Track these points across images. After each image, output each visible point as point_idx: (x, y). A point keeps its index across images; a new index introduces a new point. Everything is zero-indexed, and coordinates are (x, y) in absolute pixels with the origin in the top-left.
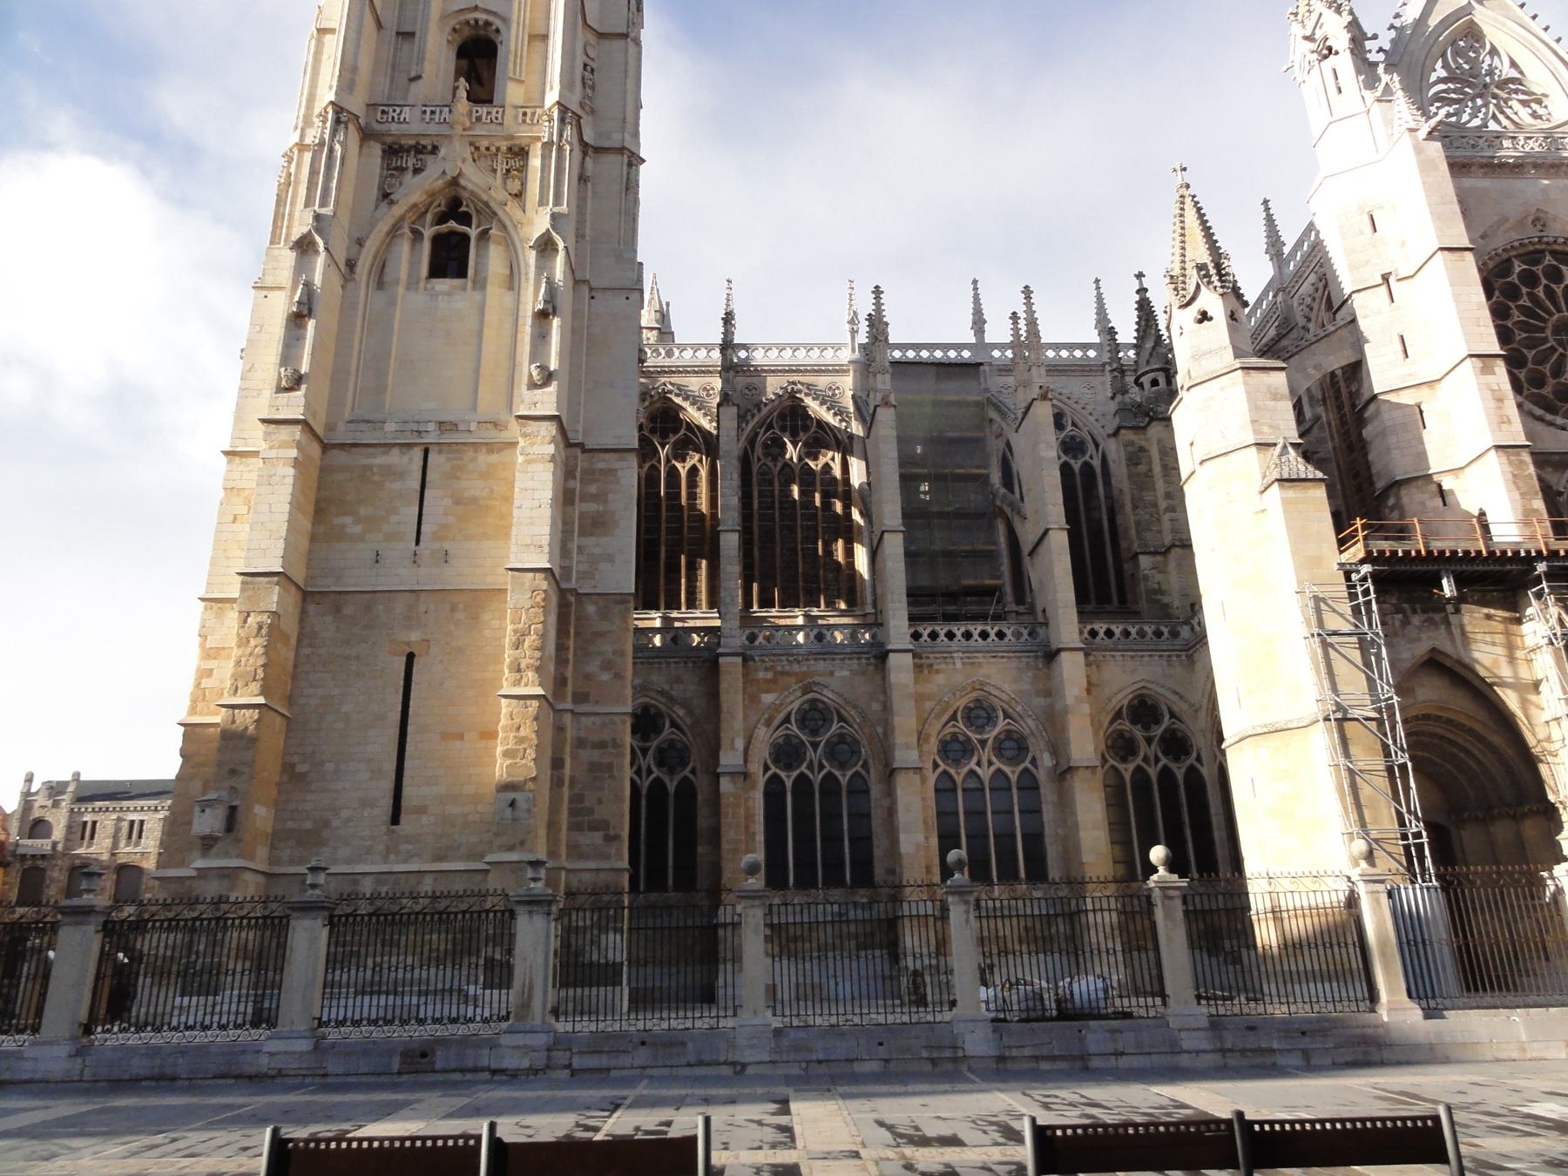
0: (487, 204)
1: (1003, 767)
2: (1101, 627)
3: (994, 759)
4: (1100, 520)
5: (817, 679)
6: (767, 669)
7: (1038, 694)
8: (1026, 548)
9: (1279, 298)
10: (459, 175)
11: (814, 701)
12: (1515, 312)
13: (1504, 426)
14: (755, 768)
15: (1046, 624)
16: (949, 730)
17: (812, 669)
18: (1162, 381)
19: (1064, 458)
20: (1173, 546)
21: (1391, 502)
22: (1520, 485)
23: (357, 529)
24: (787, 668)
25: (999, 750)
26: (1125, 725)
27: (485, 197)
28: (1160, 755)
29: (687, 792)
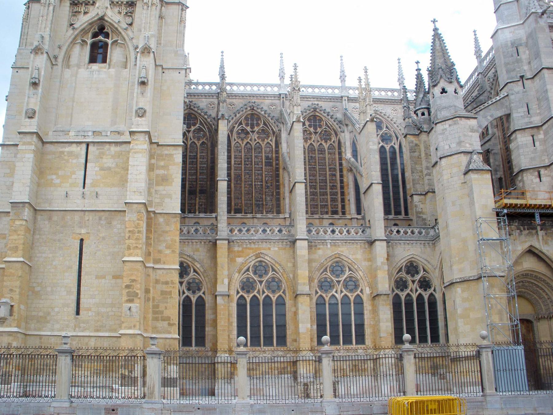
0: (117, 29)
1: (348, 294)
3: (343, 290)
4: (397, 175)
5: (262, 251)
6: (239, 246)
7: (365, 260)
8: (362, 191)
10: (104, 16)
11: (261, 261)
14: (233, 292)
15: (370, 227)
17: (260, 246)
18: (426, 113)
19: (382, 144)
20: (429, 192)
21: (520, 178)
23: (58, 181)
24: (249, 246)
25: (346, 286)
26: (403, 274)
27: (116, 26)
28: (418, 288)
29: (201, 302)
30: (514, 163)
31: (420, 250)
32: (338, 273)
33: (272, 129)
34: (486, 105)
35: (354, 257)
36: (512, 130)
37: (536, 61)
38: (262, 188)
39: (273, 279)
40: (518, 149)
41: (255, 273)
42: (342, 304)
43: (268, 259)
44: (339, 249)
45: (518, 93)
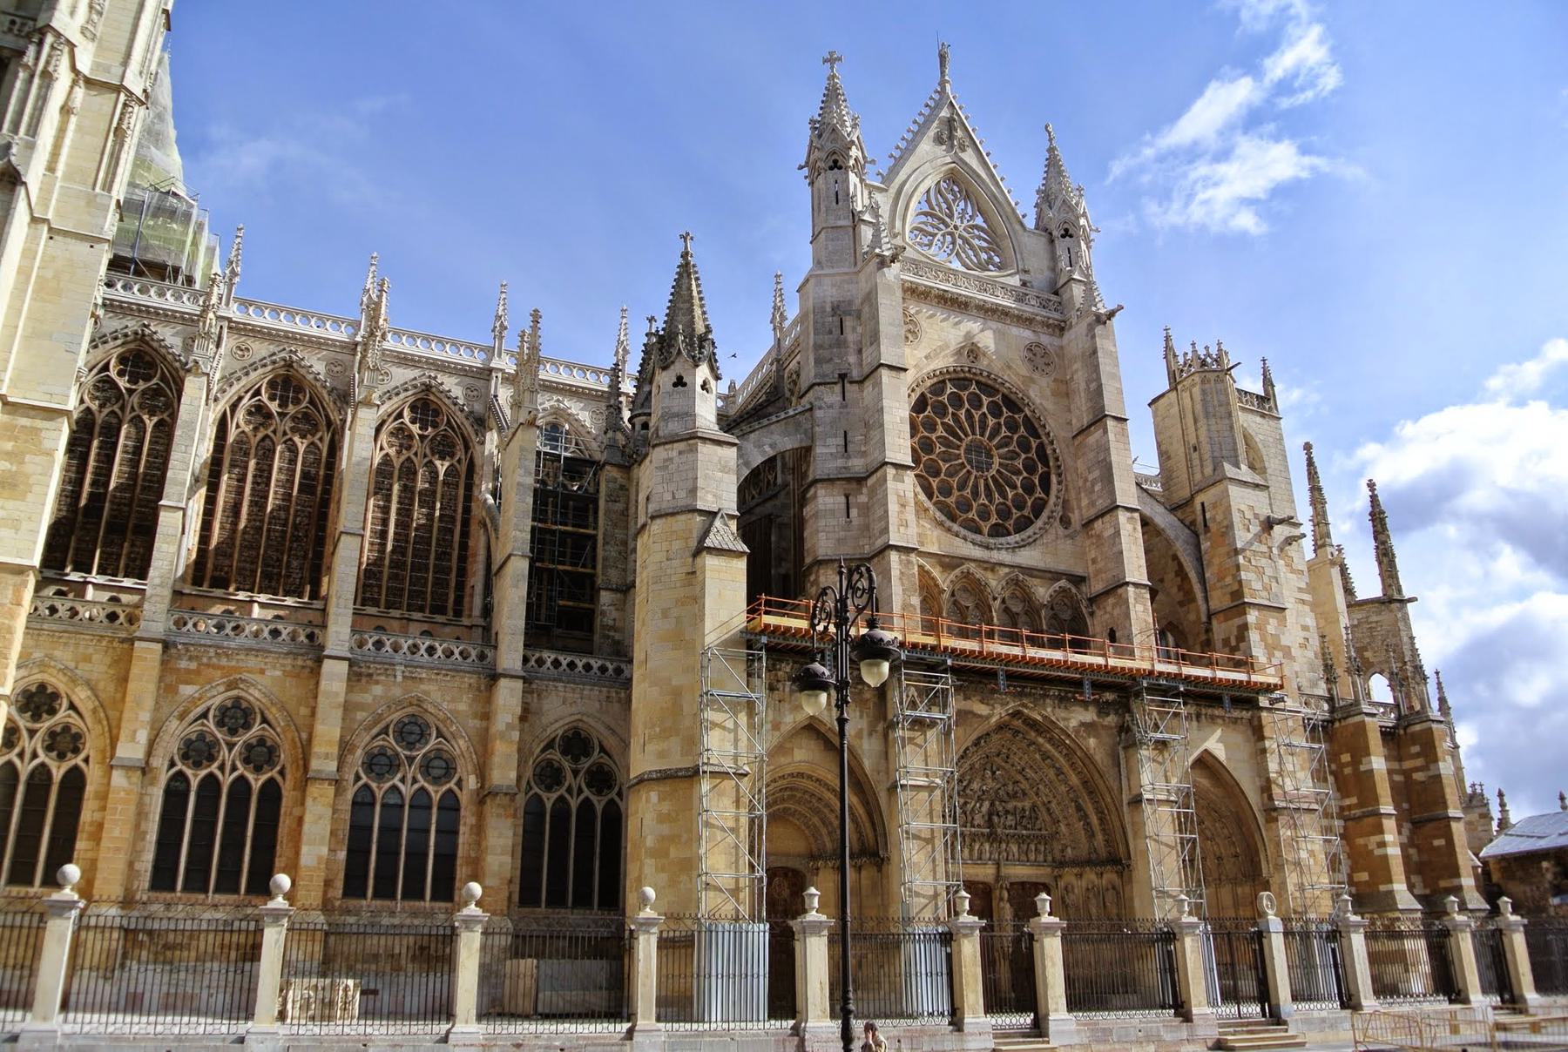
2: (548, 656)
3: (419, 777)
6: (191, 659)
7: (475, 716)
8: (495, 568)
9: (774, 368)
11: (238, 699)
12: (940, 428)
13: (902, 529)
14: (160, 762)
16: (379, 742)
17: (241, 664)
21: (812, 578)
22: (906, 582)
25: (426, 768)
26: (556, 755)
30: (807, 545)
31: (597, 705)
32: (412, 738)
33: (327, 416)
34: (765, 422)
35: (451, 706)
36: (811, 478)
37: (870, 350)
38: (284, 538)
39: (261, 741)
40: (817, 518)
41: (220, 723)
42: (410, 806)
43: (257, 694)
44: (422, 687)
45: (831, 406)
